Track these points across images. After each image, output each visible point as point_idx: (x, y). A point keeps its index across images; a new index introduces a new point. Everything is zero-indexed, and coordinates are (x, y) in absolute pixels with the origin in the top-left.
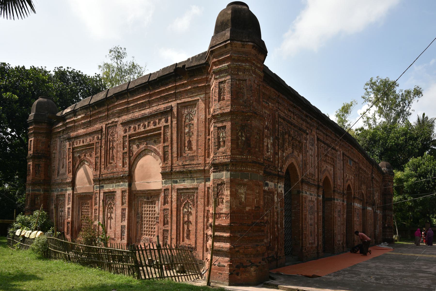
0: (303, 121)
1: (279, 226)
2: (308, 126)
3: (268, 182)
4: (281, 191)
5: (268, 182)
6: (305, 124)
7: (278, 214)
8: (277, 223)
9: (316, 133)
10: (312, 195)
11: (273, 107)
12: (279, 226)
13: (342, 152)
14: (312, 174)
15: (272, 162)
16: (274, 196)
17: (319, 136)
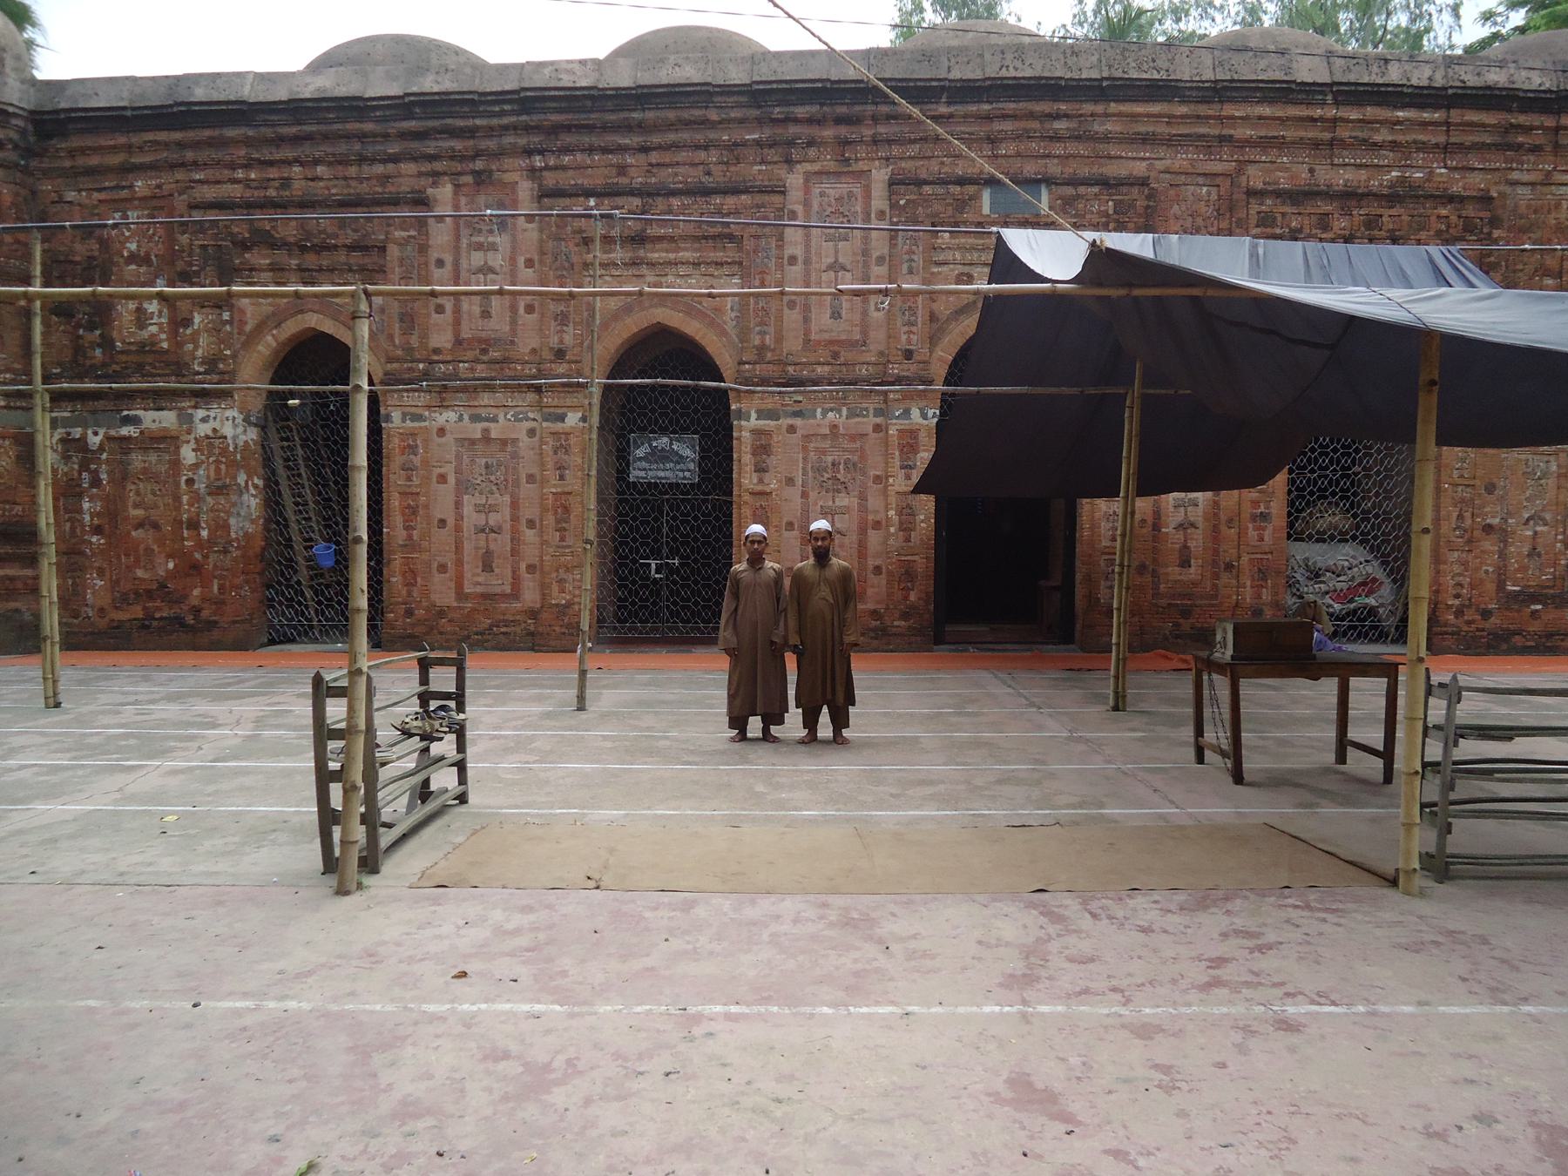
0: (395, 159)
1: (205, 533)
2: (439, 166)
3: (140, 413)
4: (215, 430)
5: (140, 413)
6: (408, 168)
7: (197, 498)
8: (194, 525)
9: (533, 172)
10: (495, 420)
11: (159, 186)
12: (205, 533)
13: (880, 176)
14: (485, 344)
15: (167, 352)
16: (178, 448)
17: (550, 179)
